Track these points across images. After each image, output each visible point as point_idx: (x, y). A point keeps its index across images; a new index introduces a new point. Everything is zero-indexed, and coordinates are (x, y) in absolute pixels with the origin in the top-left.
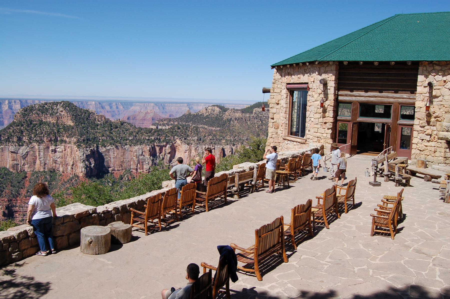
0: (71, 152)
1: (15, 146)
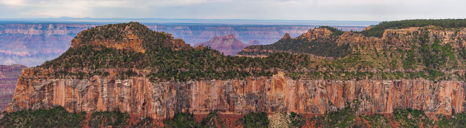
1: (73, 78)
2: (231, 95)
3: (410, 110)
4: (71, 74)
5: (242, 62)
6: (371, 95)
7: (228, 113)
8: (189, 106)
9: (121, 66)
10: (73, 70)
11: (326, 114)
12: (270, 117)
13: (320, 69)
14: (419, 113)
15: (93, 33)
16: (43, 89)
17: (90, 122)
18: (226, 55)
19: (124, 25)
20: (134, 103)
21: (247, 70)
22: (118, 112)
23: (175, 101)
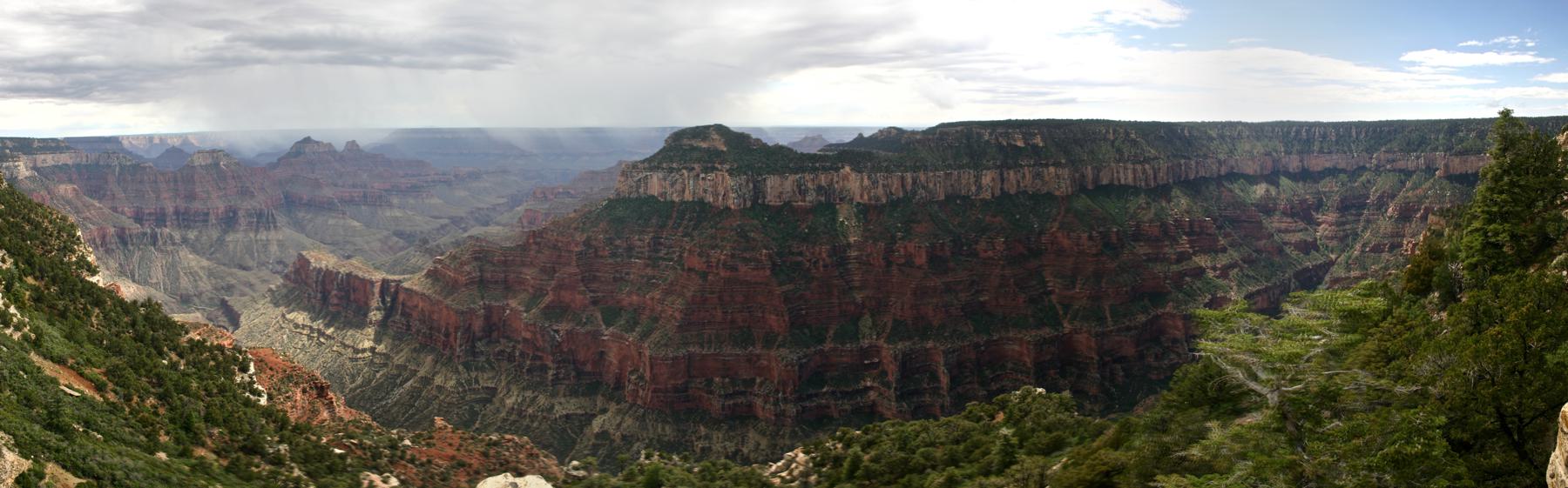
3: (958, 197)
14: (965, 198)
20: (716, 194)
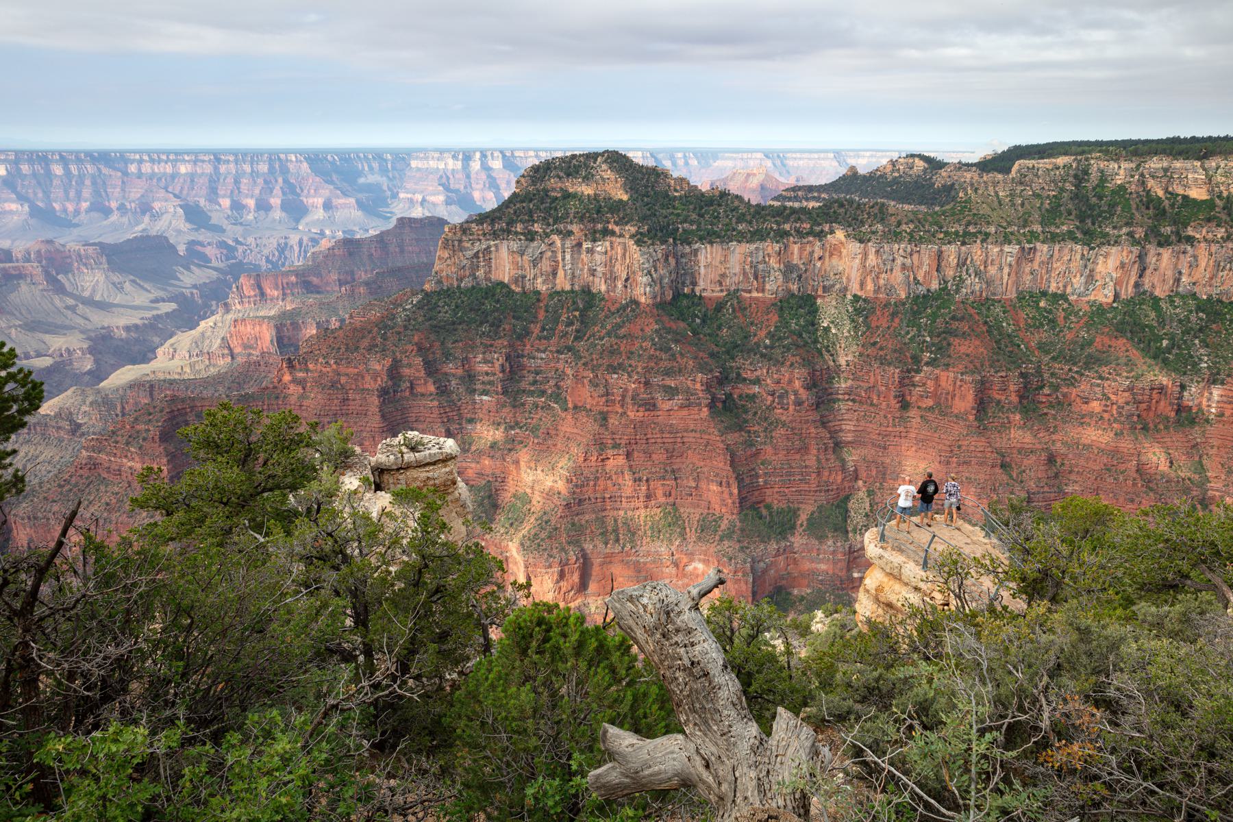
0: (624, 255)
2: (761, 267)
3: (1044, 294)
4: (516, 233)
5: (781, 214)
6: (982, 268)
7: (755, 294)
8: (694, 284)
9: (593, 220)
10: (519, 227)
11: (908, 298)
12: (819, 301)
13: (904, 227)
15: (549, 168)
16: (476, 255)
17: (546, 306)
18: (754, 202)
19: (593, 156)
20: (611, 278)
21: (787, 227)
22: (587, 291)
23: (674, 276)
